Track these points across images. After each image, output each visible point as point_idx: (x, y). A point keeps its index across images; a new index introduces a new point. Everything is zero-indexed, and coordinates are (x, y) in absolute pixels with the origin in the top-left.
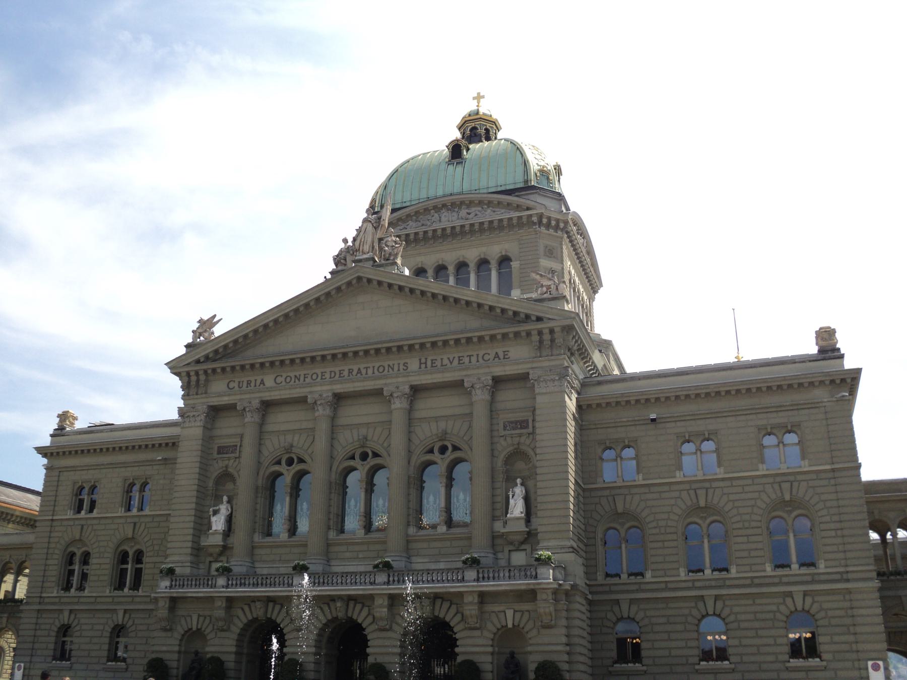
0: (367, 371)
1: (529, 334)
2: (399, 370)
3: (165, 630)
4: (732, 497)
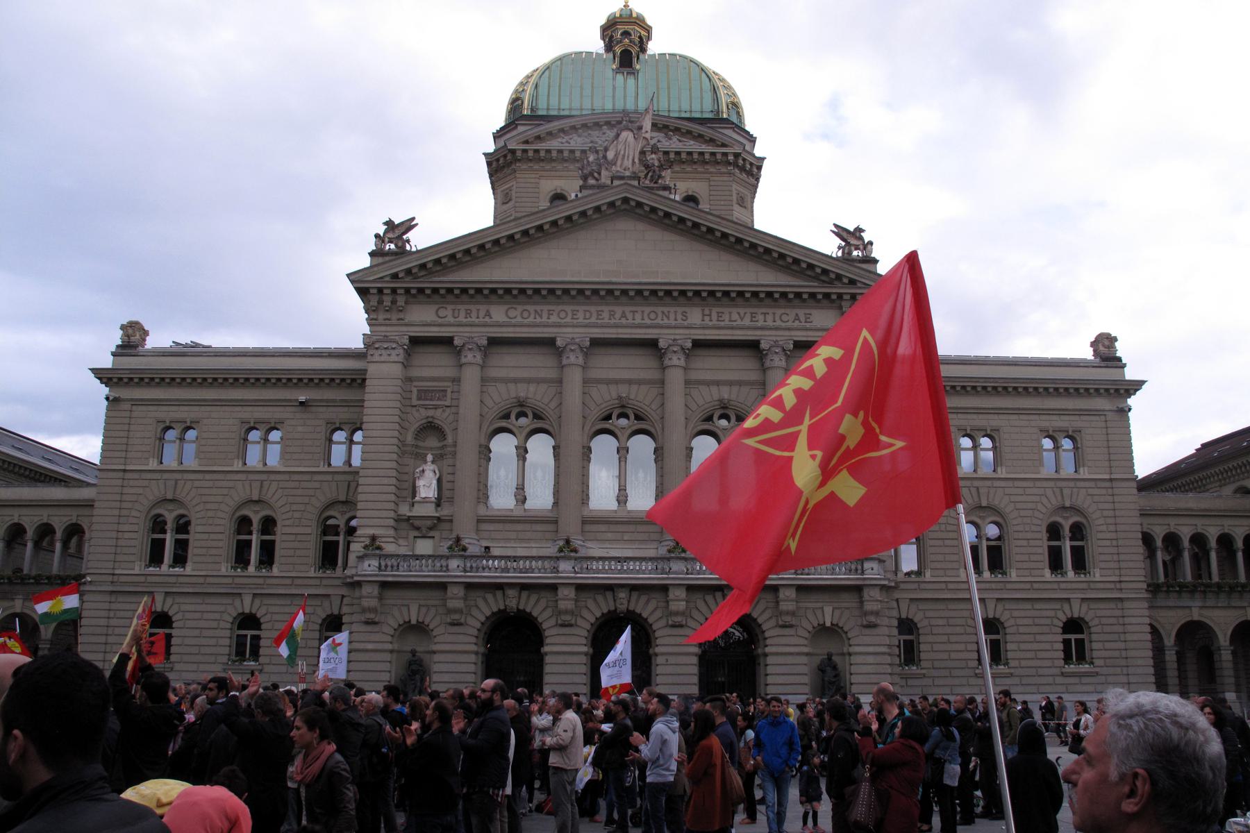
0: (634, 315)
1: (840, 296)
2: (676, 320)
3: (369, 623)
4: (1013, 498)
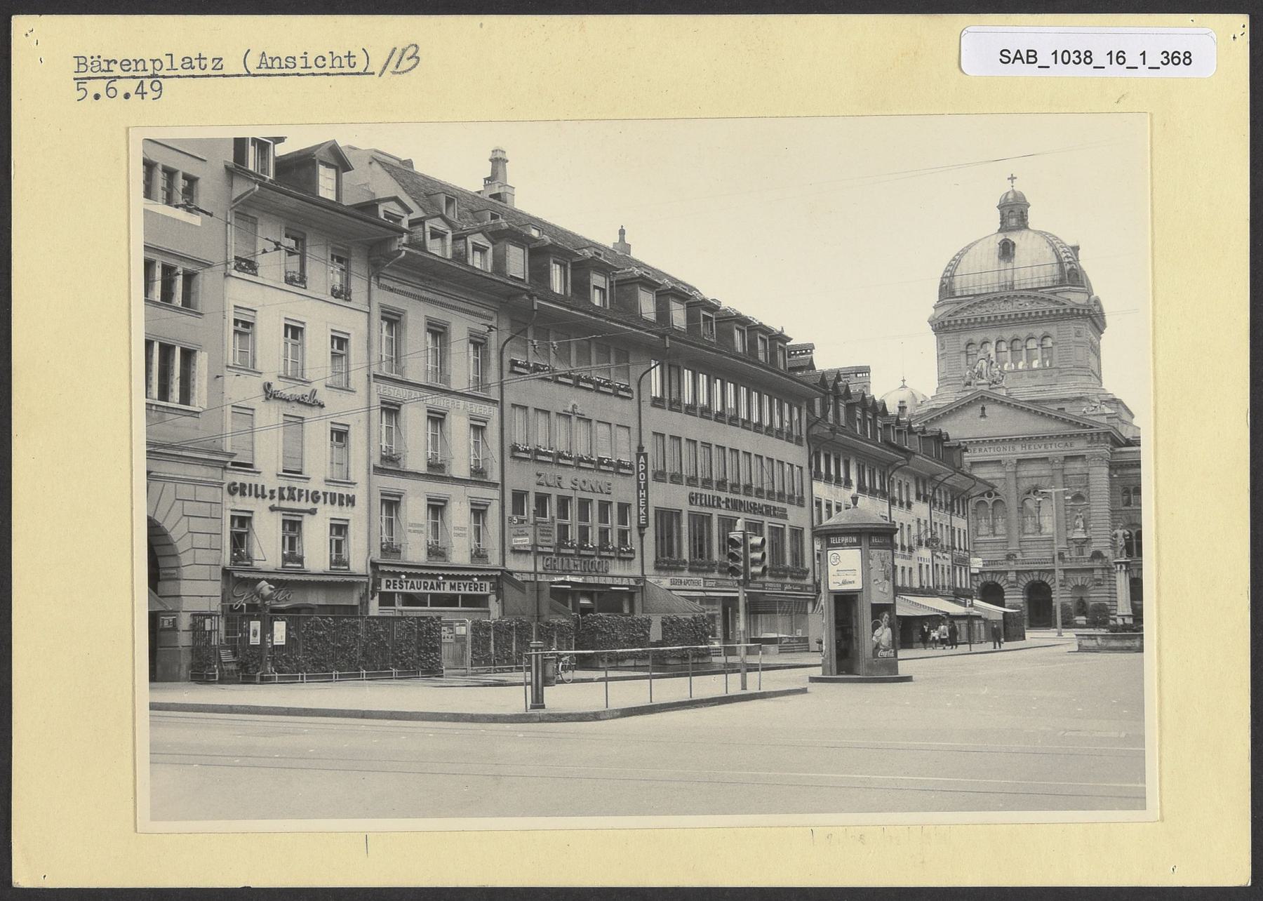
1: (1085, 434)
